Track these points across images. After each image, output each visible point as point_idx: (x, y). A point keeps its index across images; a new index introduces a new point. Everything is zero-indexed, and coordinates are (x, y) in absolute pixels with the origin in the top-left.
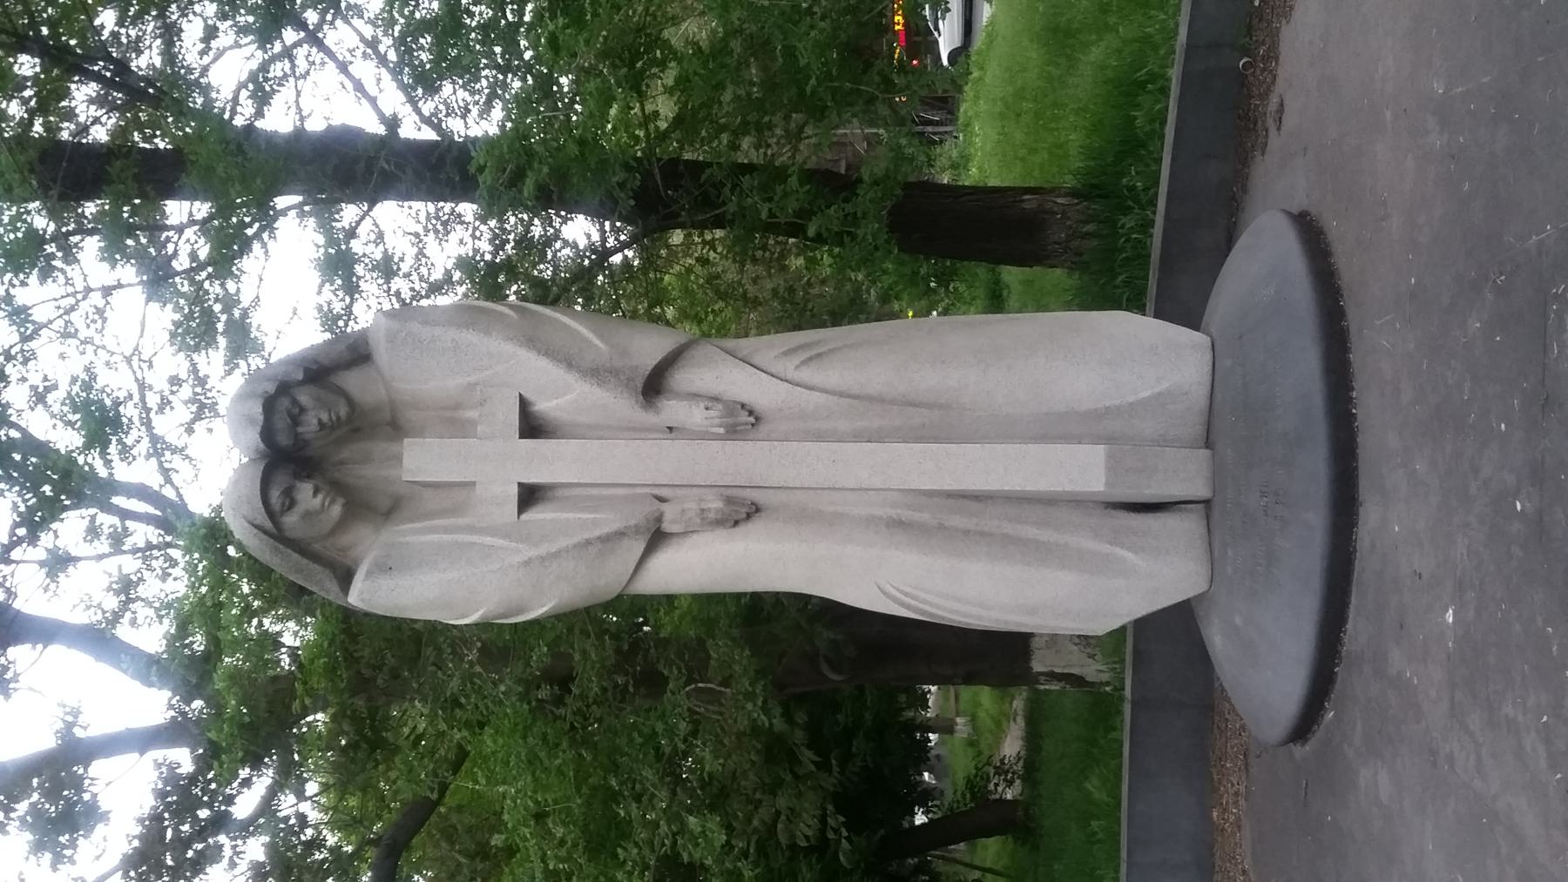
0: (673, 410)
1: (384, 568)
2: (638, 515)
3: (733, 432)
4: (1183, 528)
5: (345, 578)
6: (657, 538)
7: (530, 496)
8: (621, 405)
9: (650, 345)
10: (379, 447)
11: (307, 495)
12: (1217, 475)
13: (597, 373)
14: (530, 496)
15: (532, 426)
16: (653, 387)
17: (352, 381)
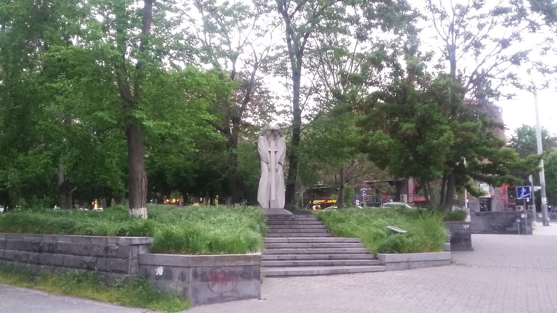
0: (278, 164)
1: (264, 139)
2: (269, 161)
3: (276, 169)
4: (268, 206)
5: (262, 135)
6: (267, 163)
7: (270, 152)
8: (278, 160)
9: (283, 163)
10: (273, 138)
11: (270, 133)
12: (272, 209)
13: (281, 158)
14: (270, 152)
15: (276, 152)
16: (280, 163)
17: (279, 135)
